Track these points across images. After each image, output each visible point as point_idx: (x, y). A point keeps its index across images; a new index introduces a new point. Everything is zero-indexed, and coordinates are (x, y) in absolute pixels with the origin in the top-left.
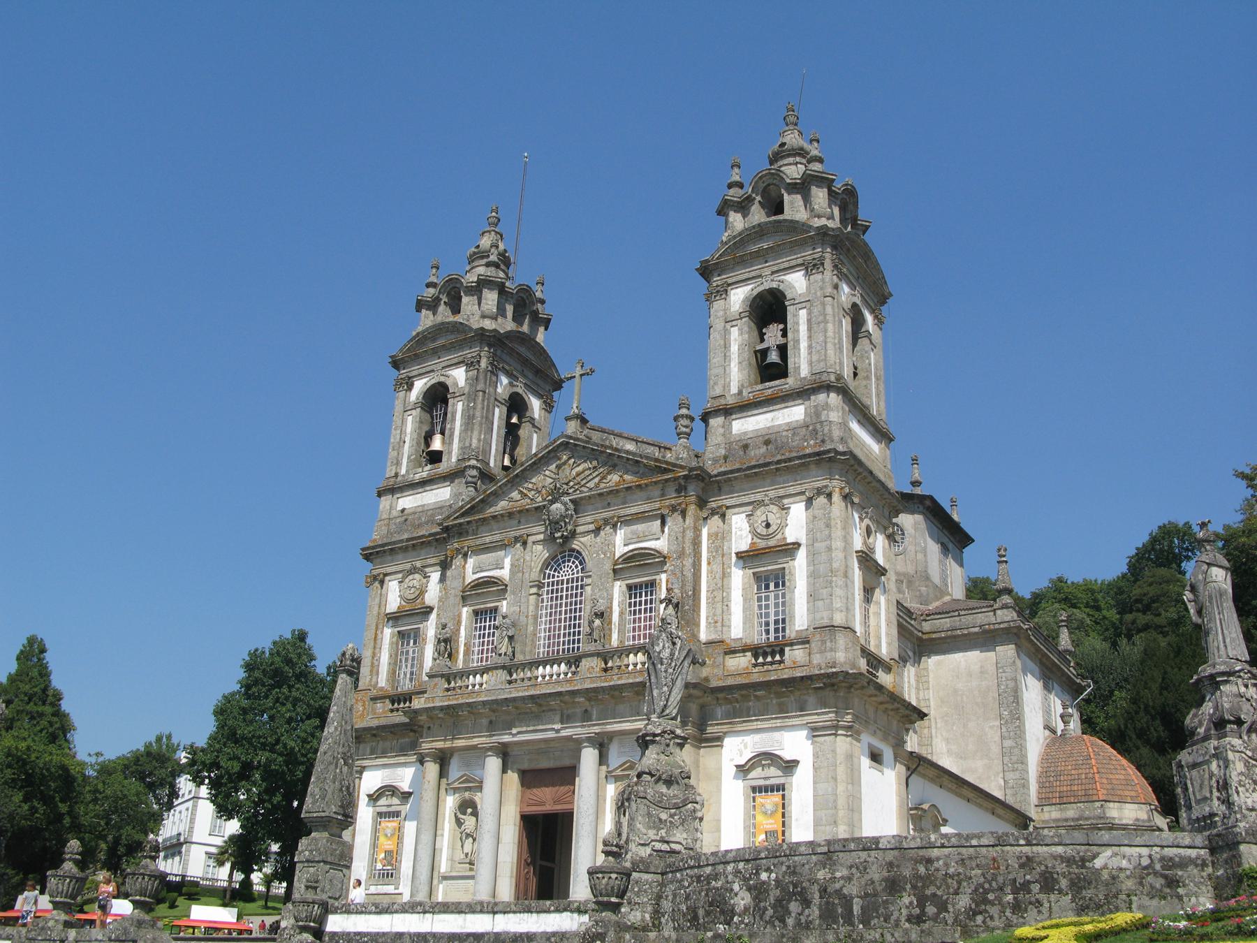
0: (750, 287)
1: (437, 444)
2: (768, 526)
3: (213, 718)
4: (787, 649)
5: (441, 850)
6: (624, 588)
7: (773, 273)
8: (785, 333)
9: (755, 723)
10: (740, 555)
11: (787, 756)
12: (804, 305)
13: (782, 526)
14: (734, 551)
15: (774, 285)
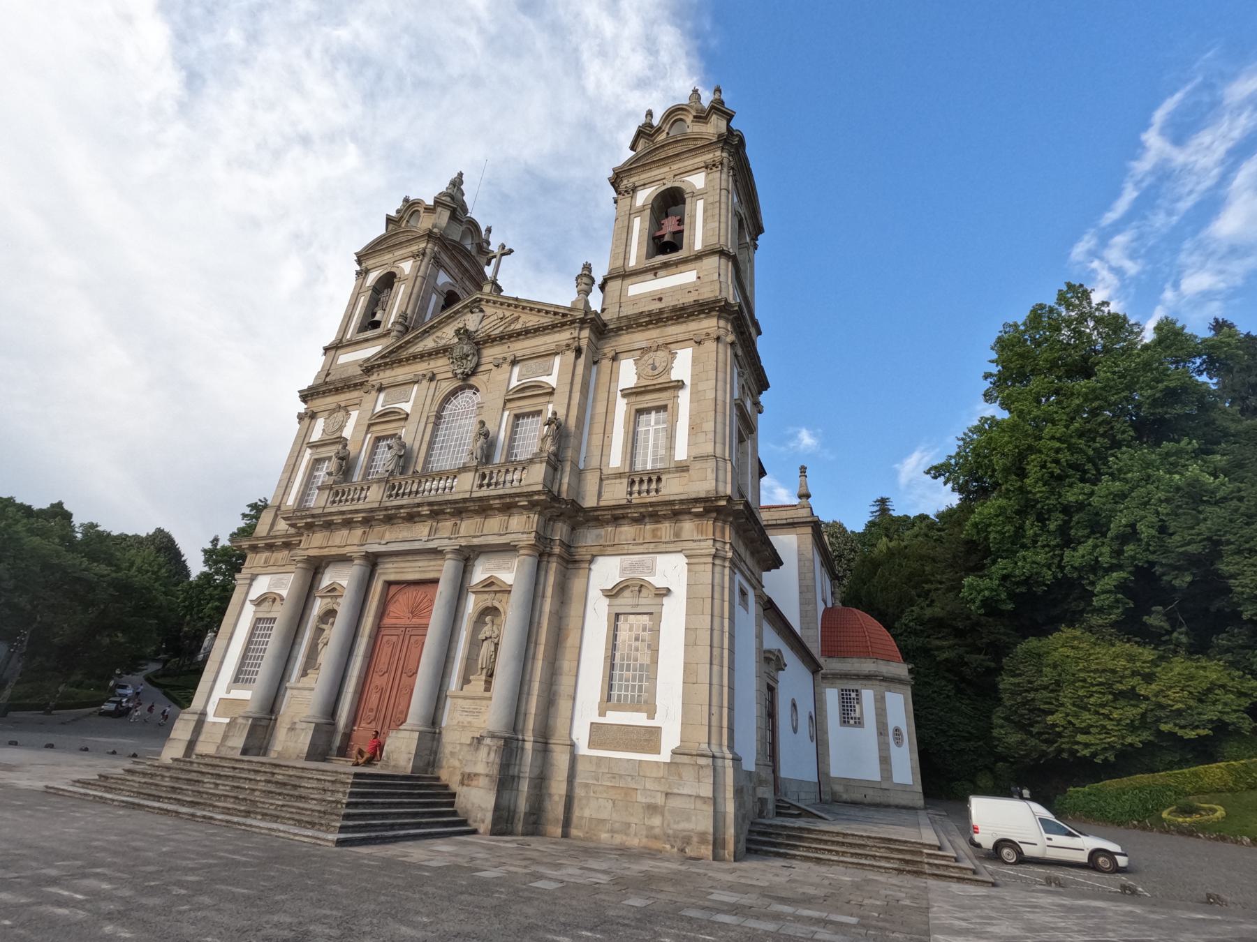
0: (654, 188)
1: (377, 317)
2: (654, 368)
3: (143, 528)
4: (664, 477)
5: (296, 658)
6: (512, 416)
7: (675, 176)
8: (681, 222)
9: (626, 546)
10: (627, 394)
11: (658, 581)
12: (701, 197)
13: (667, 369)
14: (620, 388)
15: (676, 184)
